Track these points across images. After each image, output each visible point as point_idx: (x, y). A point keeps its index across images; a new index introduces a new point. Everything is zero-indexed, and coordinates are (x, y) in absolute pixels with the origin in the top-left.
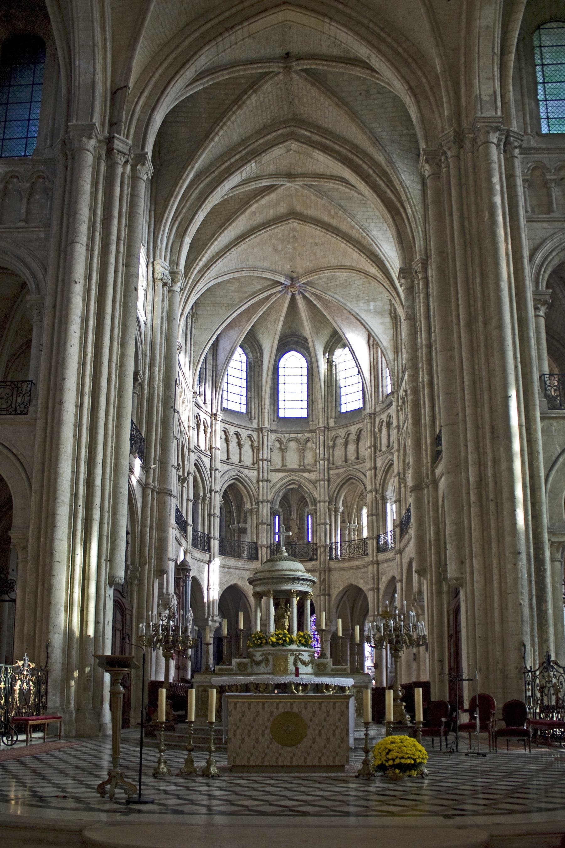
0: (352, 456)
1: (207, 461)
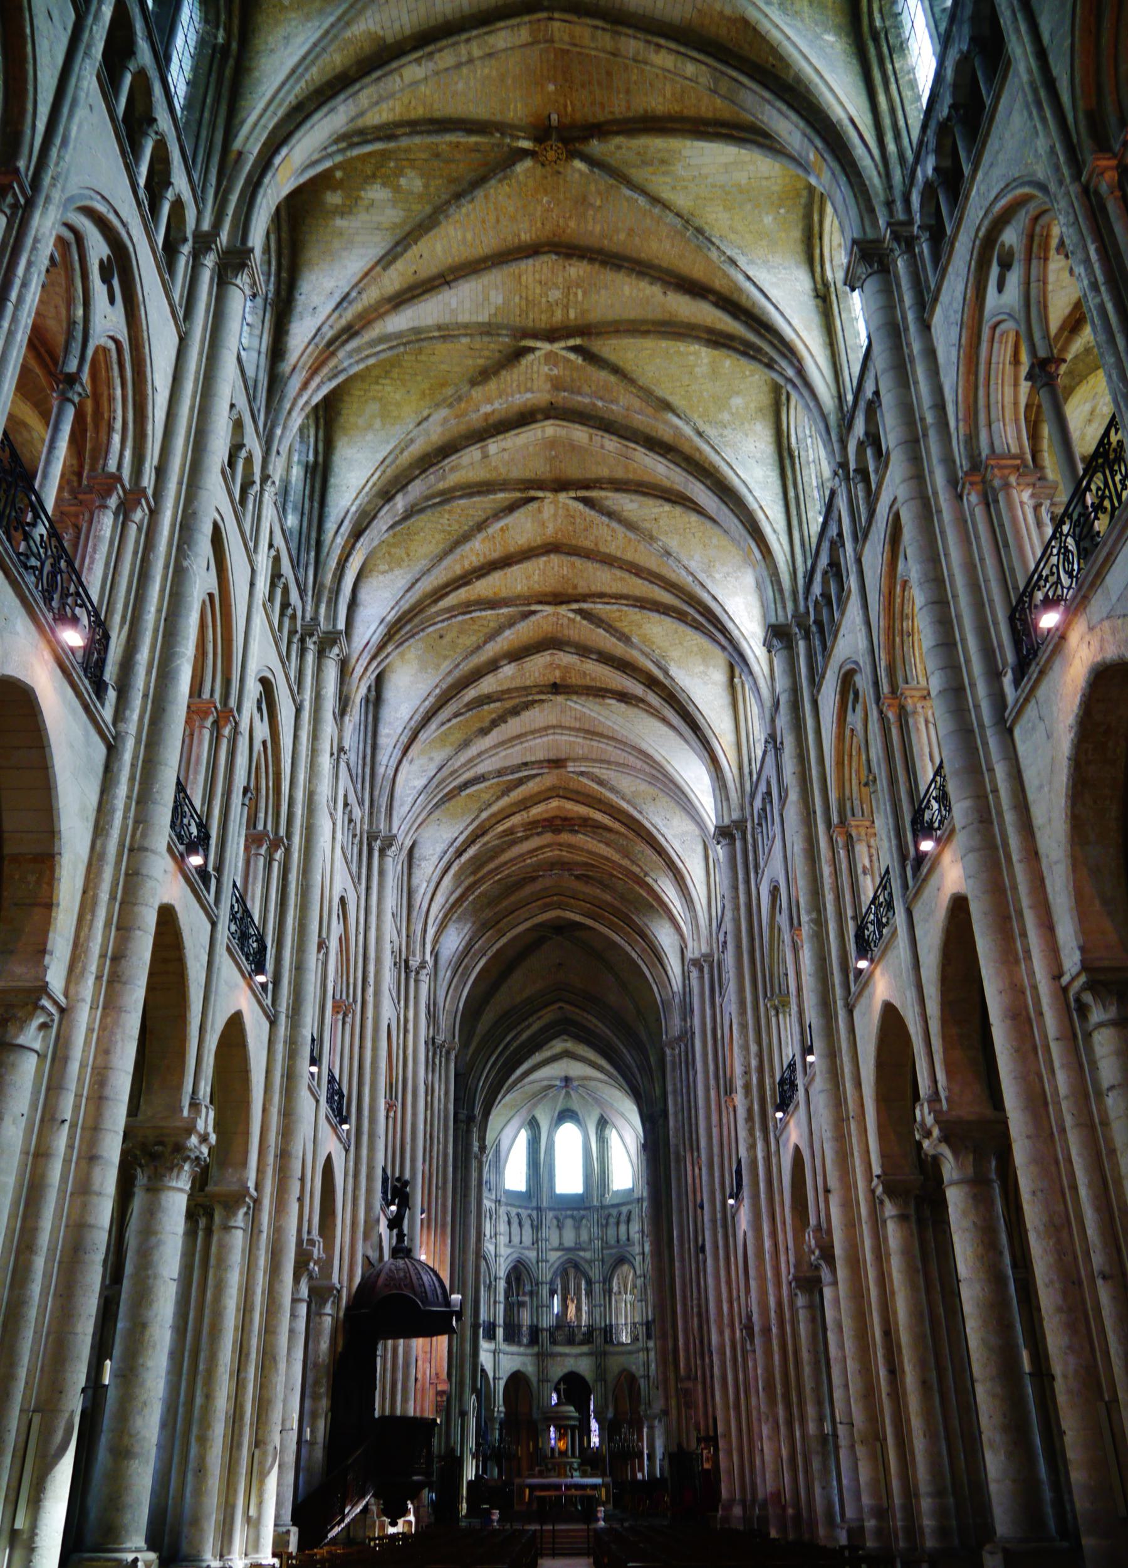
0: (623, 1237)
1: (492, 1248)
